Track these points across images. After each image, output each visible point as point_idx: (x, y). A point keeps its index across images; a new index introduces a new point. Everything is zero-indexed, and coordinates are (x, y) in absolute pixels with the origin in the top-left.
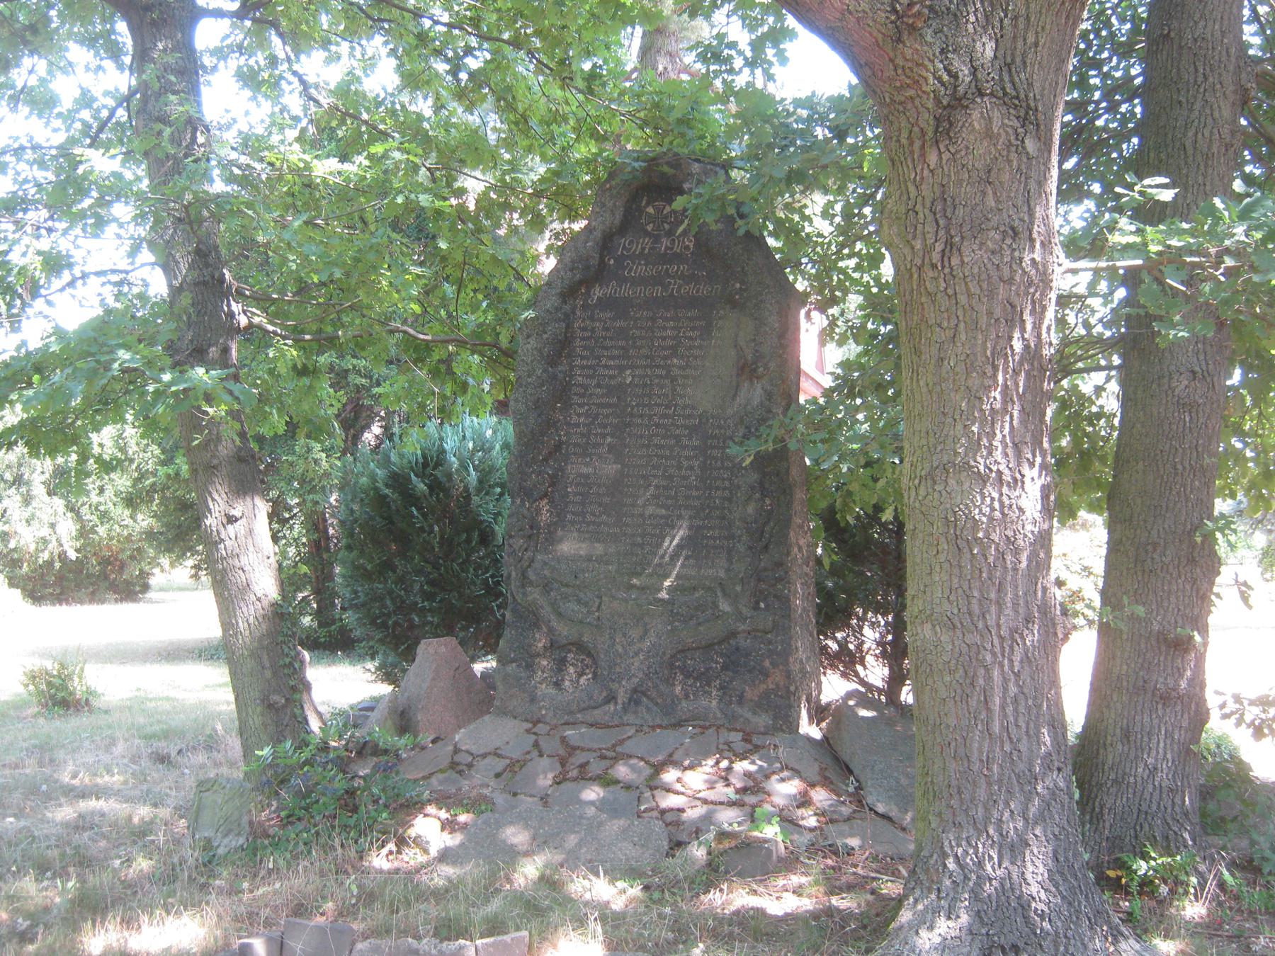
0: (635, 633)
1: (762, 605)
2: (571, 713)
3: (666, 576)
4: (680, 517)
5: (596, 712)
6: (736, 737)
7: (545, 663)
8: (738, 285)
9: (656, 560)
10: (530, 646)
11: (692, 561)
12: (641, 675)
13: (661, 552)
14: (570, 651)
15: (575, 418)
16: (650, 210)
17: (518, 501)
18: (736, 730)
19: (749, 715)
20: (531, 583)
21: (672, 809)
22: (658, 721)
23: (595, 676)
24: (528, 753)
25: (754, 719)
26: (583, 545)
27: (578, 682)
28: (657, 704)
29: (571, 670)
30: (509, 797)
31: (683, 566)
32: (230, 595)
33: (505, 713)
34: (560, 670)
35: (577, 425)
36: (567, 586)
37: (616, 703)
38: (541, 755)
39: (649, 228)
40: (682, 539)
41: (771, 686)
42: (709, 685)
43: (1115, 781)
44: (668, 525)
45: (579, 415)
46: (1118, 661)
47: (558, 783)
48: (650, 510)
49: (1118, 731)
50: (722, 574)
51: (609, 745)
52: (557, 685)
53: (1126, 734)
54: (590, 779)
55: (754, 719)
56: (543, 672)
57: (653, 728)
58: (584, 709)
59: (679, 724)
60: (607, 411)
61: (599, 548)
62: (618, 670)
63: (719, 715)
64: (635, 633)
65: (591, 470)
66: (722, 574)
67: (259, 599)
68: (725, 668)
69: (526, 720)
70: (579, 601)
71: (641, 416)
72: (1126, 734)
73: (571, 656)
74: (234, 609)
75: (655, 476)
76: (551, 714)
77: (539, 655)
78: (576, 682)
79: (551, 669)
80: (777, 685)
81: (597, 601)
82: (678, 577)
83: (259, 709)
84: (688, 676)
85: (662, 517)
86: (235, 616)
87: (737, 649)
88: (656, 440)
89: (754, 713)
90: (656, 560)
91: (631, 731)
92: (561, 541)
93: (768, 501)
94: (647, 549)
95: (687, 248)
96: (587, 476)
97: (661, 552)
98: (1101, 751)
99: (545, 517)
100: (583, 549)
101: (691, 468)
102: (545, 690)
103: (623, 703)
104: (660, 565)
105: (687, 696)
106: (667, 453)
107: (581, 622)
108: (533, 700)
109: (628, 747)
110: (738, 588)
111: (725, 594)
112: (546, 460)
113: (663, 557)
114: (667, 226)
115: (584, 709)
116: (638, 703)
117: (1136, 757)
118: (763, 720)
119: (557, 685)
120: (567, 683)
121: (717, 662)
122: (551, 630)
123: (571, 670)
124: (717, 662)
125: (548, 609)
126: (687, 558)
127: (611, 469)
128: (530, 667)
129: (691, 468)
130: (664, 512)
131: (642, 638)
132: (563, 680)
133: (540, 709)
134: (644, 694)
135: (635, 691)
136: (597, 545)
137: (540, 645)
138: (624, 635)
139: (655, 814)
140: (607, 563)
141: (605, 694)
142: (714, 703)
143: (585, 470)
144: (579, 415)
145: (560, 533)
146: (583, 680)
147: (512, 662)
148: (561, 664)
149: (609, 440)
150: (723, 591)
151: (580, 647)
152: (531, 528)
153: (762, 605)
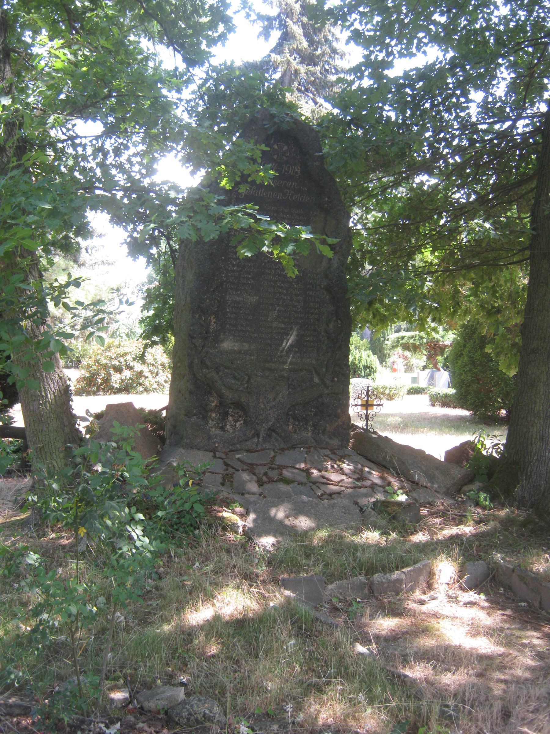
0: (271, 396)
1: (336, 379)
2: (234, 444)
3: (284, 363)
4: (292, 329)
5: (248, 443)
6: (328, 452)
7: (214, 415)
8: (326, 199)
9: (279, 354)
10: (206, 405)
11: (298, 354)
12: (273, 420)
13: (281, 349)
14: (230, 408)
15: (231, 266)
16: (276, 147)
17: (197, 316)
18: (324, 448)
19: (327, 440)
20: (207, 367)
21: (334, 493)
22: (282, 446)
23: (246, 422)
24: (227, 470)
25: (331, 442)
26: (237, 344)
27: (235, 426)
28: (281, 437)
29: (230, 419)
30: (240, 496)
31: (293, 357)
32: (42, 376)
33: (192, 448)
34: (223, 419)
35: (233, 271)
36: (229, 368)
37: (258, 437)
38: (238, 470)
39: (275, 157)
40: (293, 342)
41: (340, 423)
42: (306, 424)
43: (537, 459)
44: (286, 333)
45: (234, 265)
46: (538, 404)
47: (262, 485)
48: (275, 324)
49: (538, 437)
50: (314, 362)
51: (268, 461)
52: (223, 428)
53: (542, 438)
54: (276, 481)
55: (331, 442)
56: (213, 421)
57: (283, 450)
58: (241, 442)
59: (293, 447)
60: (250, 264)
61: (246, 346)
62: (261, 418)
63: (313, 441)
64: (271, 396)
65: (241, 299)
66: (314, 362)
67: (61, 378)
68: (316, 414)
69: (207, 451)
70: (235, 378)
71: (270, 268)
72: (542, 438)
73: (231, 410)
74: (44, 385)
75: (278, 305)
76: (221, 446)
77: (211, 411)
78: (234, 426)
79: (218, 419)
80: (343, 422)
81: (247, 378)
82: (291, 363)
83: (62, 455)
84: (296, 418)
85: (282, 329)
86: (45, 390)
87: (323, 404)
88: (279, 284)
89: (330, 438)
90: (279, 354)
91: (272, 454)
92: (222, 341)
93: (339, 322)
94: (274, 347)
95: (297, 173)
96: (238, 303)
97: (281, 349)
98: (529, 447)
99: (213, 326)
100: (236, 346)
101: (298, 301)
102: (214, 431)
103: (263, 437)
104: (281, 356)
105: (295, 432)
106: (285, 291)
107: (237, 390)
108: (210, 438)
109: (279, 460)
110: (324, 370)
111: (318, 374)
112: (214, 291)
113: (282, 351)
114: (285, 158)
115: (241, 442)
116: (269, 436)
117: (545, 448)
118: (335, 442)
119: (223, 428)
120: (228, 427)
121: (311, 411)
122: (221, 396)
123: (230, 419)
124: (311, 411)
125: (220, 383)
126: (296, 352)
127: (253, 299)
128: (205, 418)
129: (298, 301)
130: (283, 326)
131: (275, 399)
132: (226, 425)
133: (214, 443)
134: (274, 431)
135: (270, 429)
136: (244, 344)
137: (213, 404)
138: (265, 397)
139: (326, 496)
140: (251, 355)
141: (253, 432)
142: (310, 434)
143: (237, 299)
144: (234, 265)
145: (222, 336)
146: (238, 424)
147: (195, 415)
148: (225, 415)
149: (252, 281)
150: (316, 371)
151: (238, 405)
152: (206, 333)
153: (336, 379)
